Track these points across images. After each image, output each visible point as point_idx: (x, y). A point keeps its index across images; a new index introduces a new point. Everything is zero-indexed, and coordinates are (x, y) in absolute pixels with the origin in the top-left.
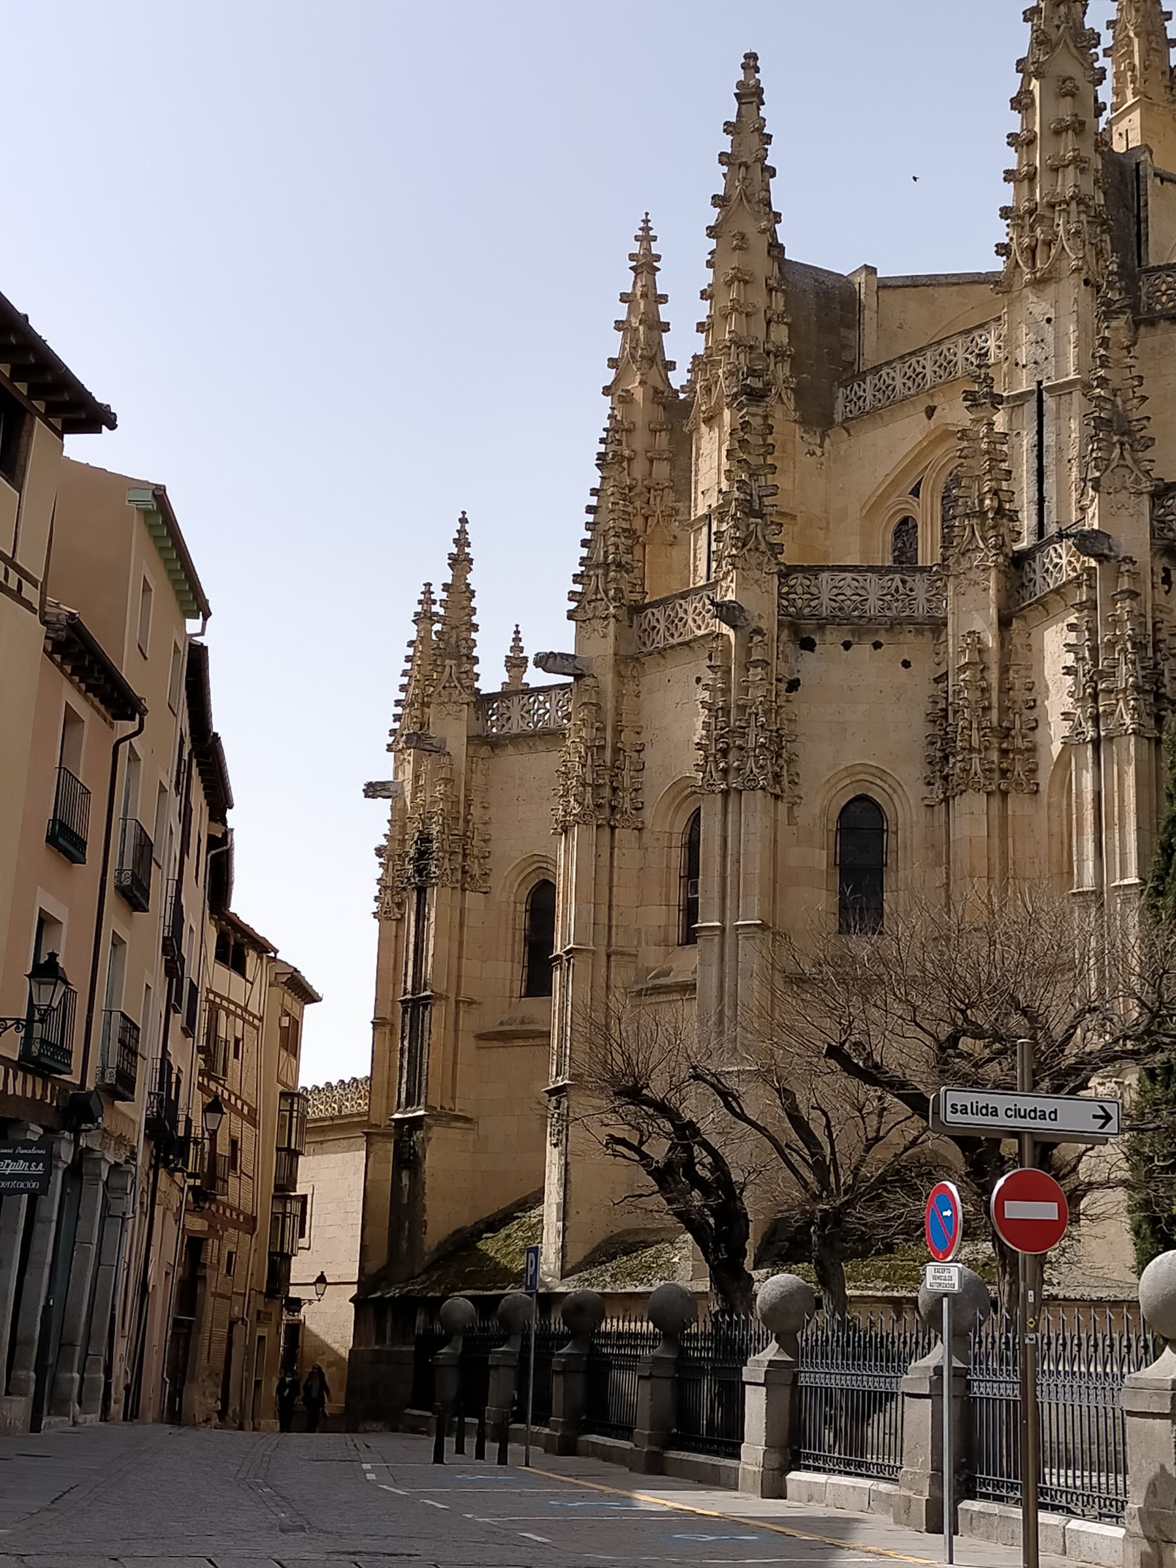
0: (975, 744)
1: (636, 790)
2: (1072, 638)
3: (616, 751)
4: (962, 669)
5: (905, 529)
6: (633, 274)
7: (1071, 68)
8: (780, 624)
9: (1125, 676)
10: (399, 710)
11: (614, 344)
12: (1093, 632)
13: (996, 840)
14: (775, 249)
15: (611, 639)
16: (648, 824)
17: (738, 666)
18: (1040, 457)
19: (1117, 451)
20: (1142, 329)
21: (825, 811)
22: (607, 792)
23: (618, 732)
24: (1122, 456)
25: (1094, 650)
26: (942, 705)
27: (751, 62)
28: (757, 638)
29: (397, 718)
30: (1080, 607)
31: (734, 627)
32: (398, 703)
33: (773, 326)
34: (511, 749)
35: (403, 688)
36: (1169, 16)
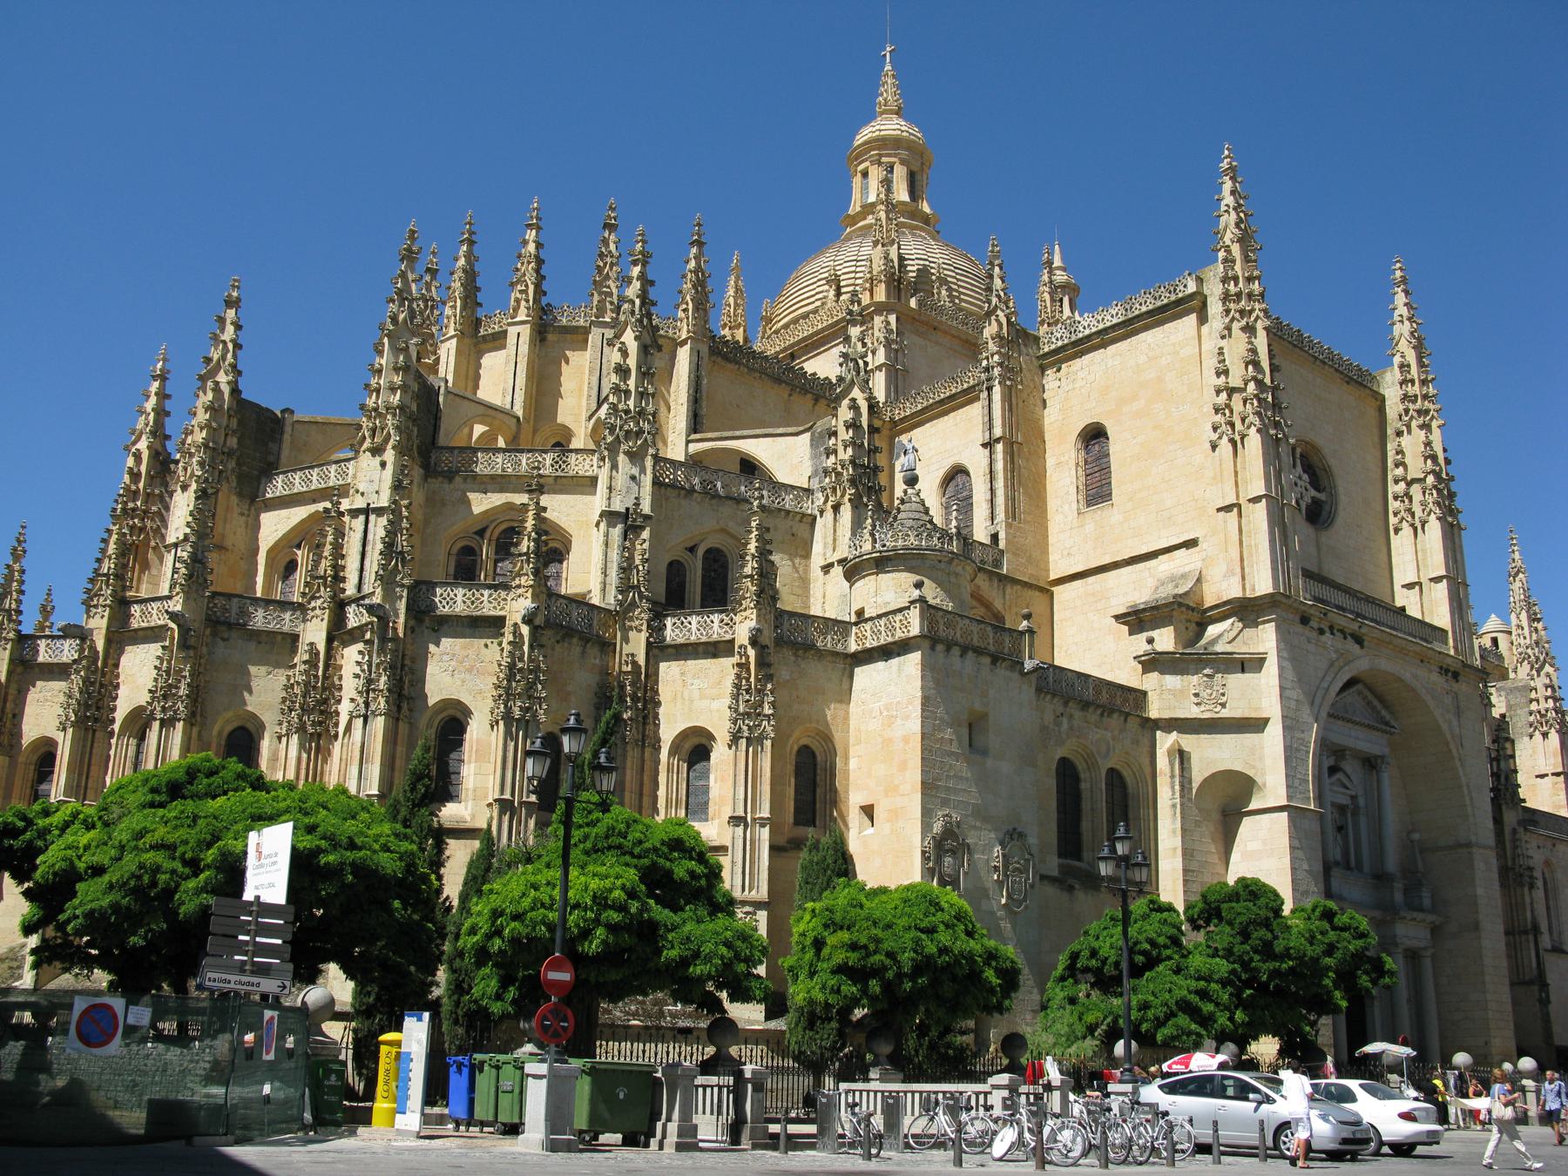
2: (359, 658)
3: (102, 685)
4: (305, 662)
9: (383, 682)
12: (371, 657)
15: (105, 620)
16: (117, 731)
18: (364, 546)
21: (220, 733)
23: (104, 674)
24: (396, 564)
25: (370, 666)
30: (366, 642)
31: (179, 626)
33: (229, 438)
36: (478, 289)
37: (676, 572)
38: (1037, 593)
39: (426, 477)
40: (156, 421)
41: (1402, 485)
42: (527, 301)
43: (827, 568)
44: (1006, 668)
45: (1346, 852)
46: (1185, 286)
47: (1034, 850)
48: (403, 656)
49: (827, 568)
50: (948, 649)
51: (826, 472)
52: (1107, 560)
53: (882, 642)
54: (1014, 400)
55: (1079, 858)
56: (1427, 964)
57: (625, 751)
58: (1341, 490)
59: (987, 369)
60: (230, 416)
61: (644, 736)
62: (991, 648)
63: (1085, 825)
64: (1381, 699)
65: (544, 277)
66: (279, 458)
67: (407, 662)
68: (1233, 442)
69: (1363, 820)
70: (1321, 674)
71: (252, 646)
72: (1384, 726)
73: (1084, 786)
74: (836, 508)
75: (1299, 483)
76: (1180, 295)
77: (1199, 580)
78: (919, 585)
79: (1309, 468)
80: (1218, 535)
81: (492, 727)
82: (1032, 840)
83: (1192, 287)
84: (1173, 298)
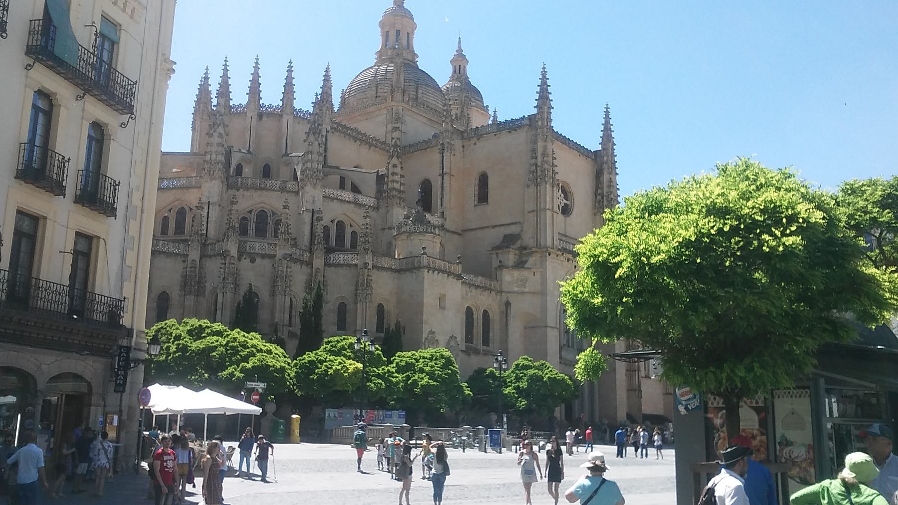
0: (193, 284)
5: (166, 219)
26: (185, 274)
37: (326, 229)
38: (457, 236)
41: (599, 198)
43: (383, 229)
45: (568, 341)
49: (383, 229)
50: (433, 272)
51: (385, 192)
52: (486, 225)
55: (472, 343)
58: (576, 200)
63: (475, 331)
73: (474, 317)
79: (564, 192)
81: (270, 296)
82: (459, 339)
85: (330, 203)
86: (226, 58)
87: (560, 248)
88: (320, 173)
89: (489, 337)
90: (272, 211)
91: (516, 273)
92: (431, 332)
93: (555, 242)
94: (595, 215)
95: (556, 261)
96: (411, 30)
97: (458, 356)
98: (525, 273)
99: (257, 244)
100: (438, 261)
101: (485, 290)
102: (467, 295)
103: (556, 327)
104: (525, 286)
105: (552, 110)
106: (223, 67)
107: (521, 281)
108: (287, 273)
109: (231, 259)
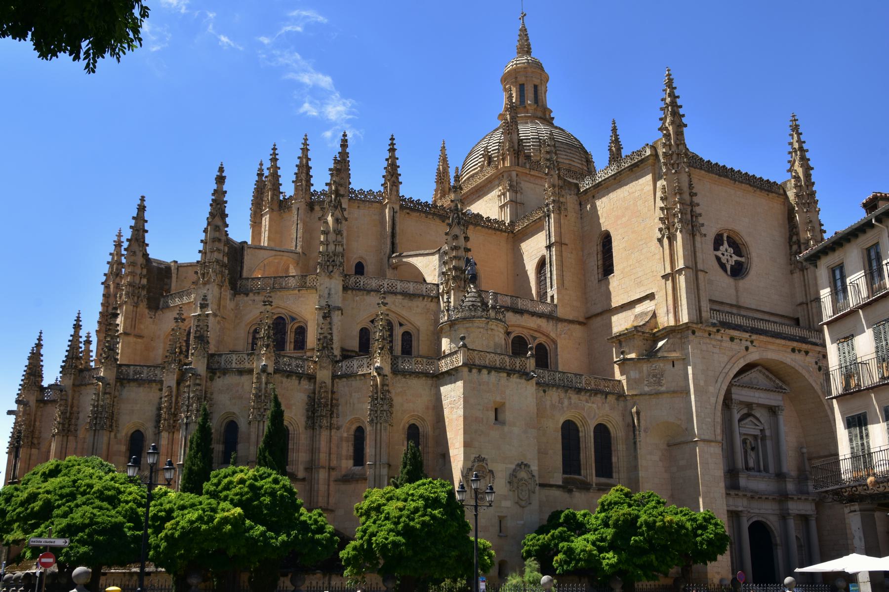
1: (76, 425)
3: (71, 413)
4: (166, 397)
6: (114, 247)
7: (220, 223)
8: (116, 382)
10: (20, 387)
11: (106, 269)
13: (170, 446)
14: (146, 255)
15: (71, 381)
17: (102, 393)
19: (199, 346)
20: (237, 296)
21: (126, 434)
22: (66, 426)
23: (72, 407)
27: (143, 199)
28: (108, 386)
29: (19, 390)
32: (20, 385)
33: (142, 279)
34: (50, 405)
35: (22, 380)
36: (281, 185)
38: (578, 326)
39: (234, 295)
40: (117, 269)
41: (795, 247)
42: (302, 190)
44: (517, 378)
46: (645, 152)
47: (536, 473)
48: (206, 392)
53: (449, 368)
54: (562, 221)
55: (580, 474)
56: (813, 524)
57: (320, 432)
58: (754, 255)
59: (547, 205)
60: (142, 268)
61: (331, 424)
62: (508, 368)
64: (777, 375)
65: (312, 176)
66: (170, 287)
67: (208, 395)
68: (669, 238)
69: (769, 444)
70: (723, 365)
71: (141, 389)
72: (778, 390)
73: (581, 434)
74: (448, 293)
75: (726, 253)
76: (643, 157)
77: (654, 315)
78: (463, 338)
80: (662, 290)
82: (534, 468)
83: (648, 152)
84: (640, 158)
85: (365, 297)
86: (275, 145)
87: (715, 321)
88: (338, 256)
89: (611, 463)
90: (290, 316)
91: (645, 367)
92: (480, 459)
93: (704, 314)
94: (792, 274)
95: (708, 341)
96: (539, 81)
97: (534, 492)
98: (662, 365)
99: (234, 356)
100: (489, 356)
101: (596, 394)
102: (561, 402)
103: (716, 441)
104: (660, 385)
105: (685, 129)
106: (271, 157)
107: (654, 376)
108: (266, 391)
109: (196, 379)
